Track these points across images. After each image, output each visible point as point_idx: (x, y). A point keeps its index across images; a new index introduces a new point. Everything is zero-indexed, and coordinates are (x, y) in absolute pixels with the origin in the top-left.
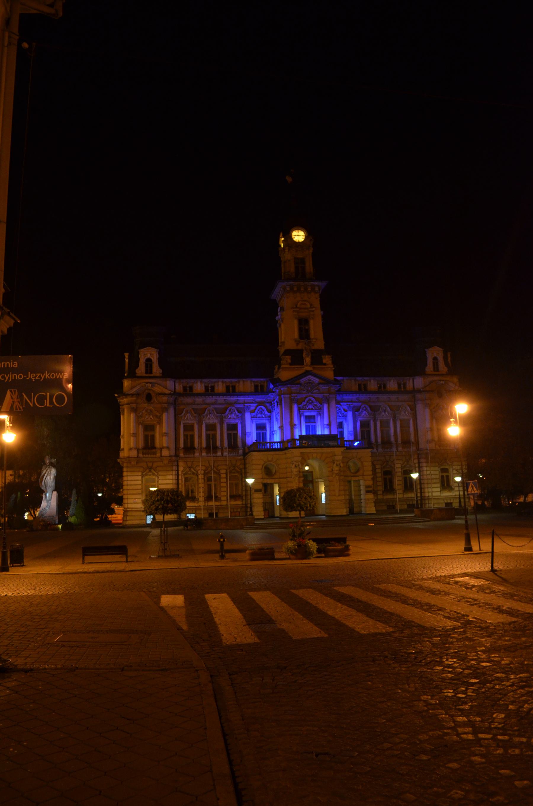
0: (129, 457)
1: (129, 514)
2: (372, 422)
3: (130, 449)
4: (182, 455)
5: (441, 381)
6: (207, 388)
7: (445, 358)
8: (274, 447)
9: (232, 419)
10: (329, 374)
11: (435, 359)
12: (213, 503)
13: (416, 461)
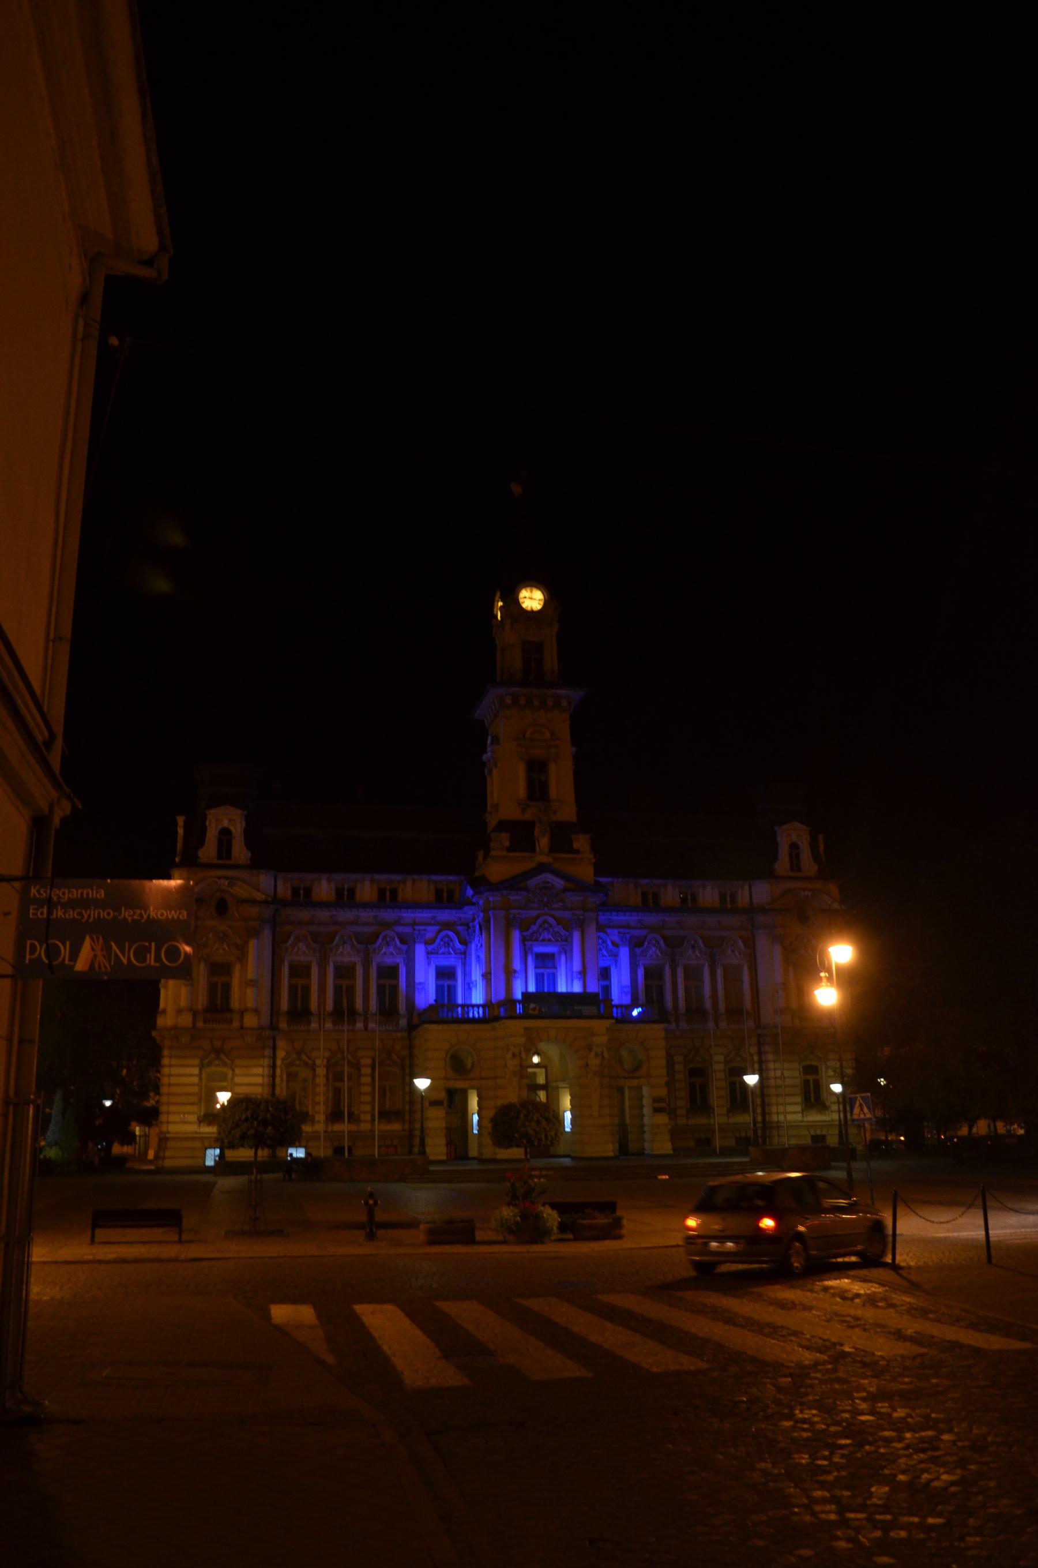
0: (175, 1028)
1: (170, 1144)
2: (667, 970)
3: (179, 1011)
4: (283, 1025)
5: (804, 890)
6: (339, 893)
7: (813, 846)
8: (471, 1015)
9: (387, 955)
10: (586, 872)
11: (794, 846)
12: (344, 1127)
13: (754, 1050)
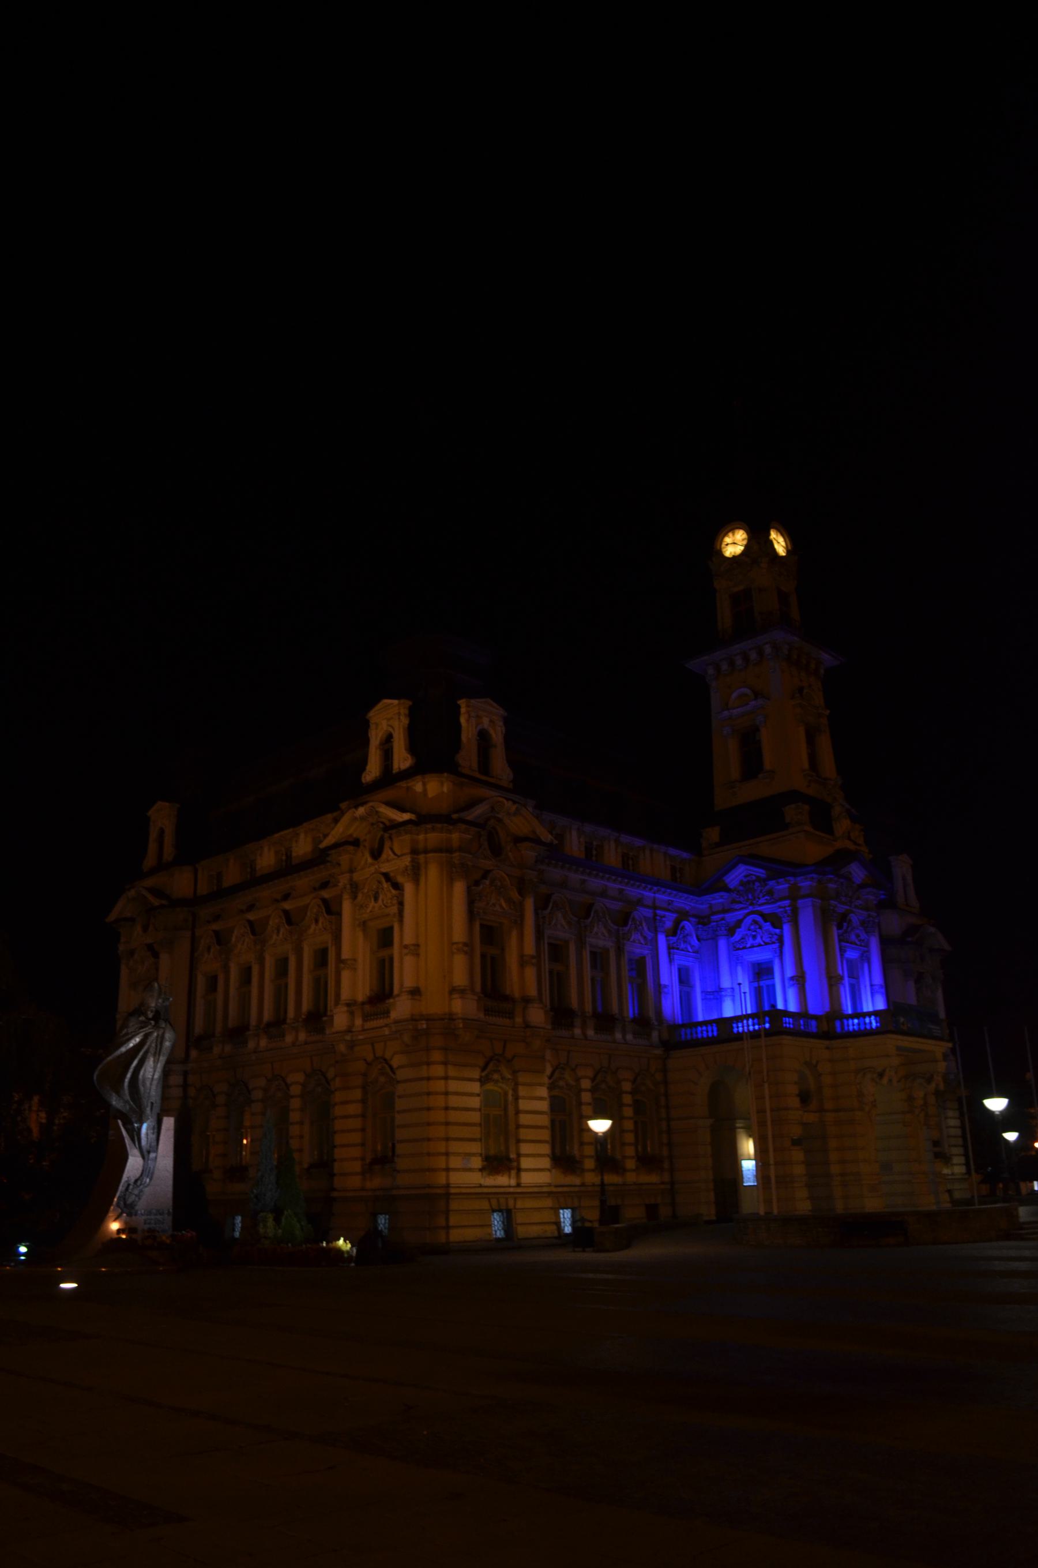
12: (611, 1178)
